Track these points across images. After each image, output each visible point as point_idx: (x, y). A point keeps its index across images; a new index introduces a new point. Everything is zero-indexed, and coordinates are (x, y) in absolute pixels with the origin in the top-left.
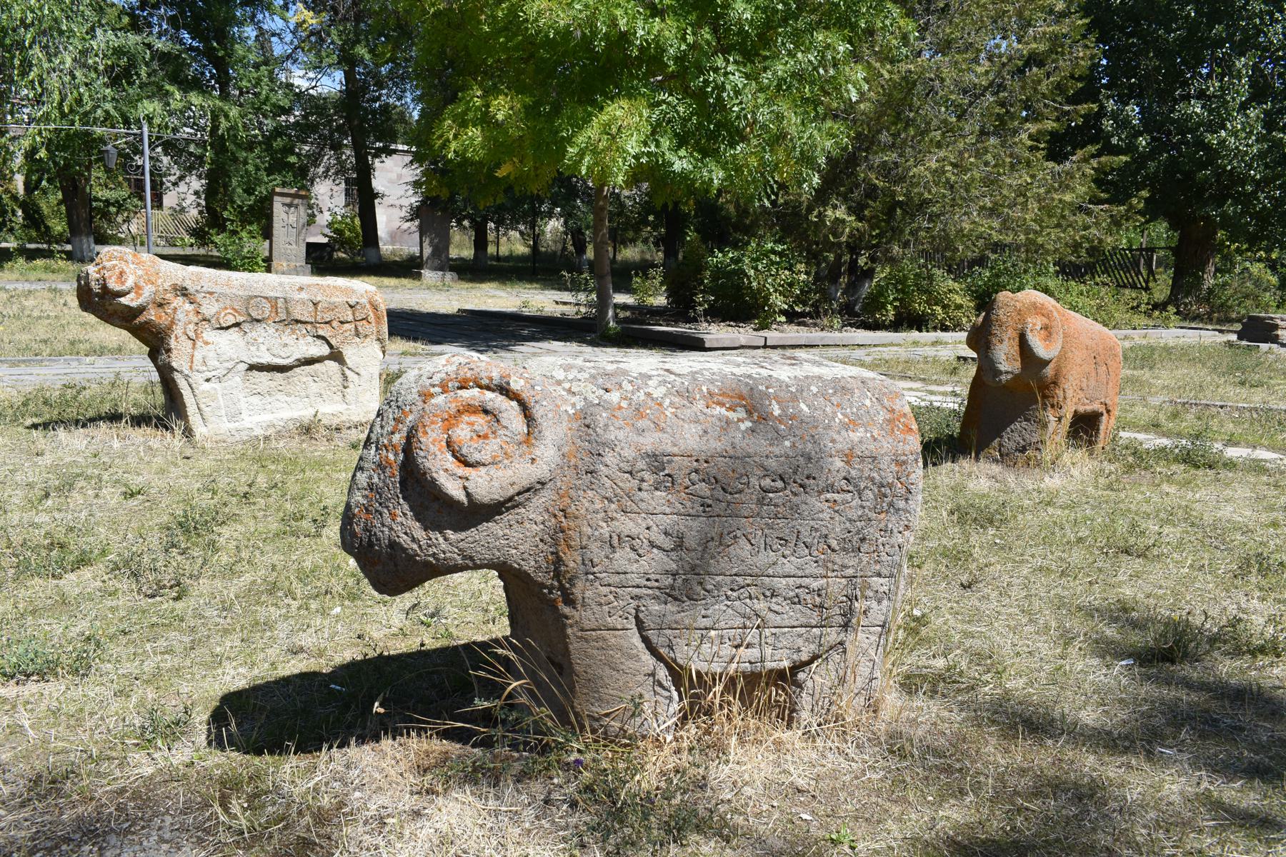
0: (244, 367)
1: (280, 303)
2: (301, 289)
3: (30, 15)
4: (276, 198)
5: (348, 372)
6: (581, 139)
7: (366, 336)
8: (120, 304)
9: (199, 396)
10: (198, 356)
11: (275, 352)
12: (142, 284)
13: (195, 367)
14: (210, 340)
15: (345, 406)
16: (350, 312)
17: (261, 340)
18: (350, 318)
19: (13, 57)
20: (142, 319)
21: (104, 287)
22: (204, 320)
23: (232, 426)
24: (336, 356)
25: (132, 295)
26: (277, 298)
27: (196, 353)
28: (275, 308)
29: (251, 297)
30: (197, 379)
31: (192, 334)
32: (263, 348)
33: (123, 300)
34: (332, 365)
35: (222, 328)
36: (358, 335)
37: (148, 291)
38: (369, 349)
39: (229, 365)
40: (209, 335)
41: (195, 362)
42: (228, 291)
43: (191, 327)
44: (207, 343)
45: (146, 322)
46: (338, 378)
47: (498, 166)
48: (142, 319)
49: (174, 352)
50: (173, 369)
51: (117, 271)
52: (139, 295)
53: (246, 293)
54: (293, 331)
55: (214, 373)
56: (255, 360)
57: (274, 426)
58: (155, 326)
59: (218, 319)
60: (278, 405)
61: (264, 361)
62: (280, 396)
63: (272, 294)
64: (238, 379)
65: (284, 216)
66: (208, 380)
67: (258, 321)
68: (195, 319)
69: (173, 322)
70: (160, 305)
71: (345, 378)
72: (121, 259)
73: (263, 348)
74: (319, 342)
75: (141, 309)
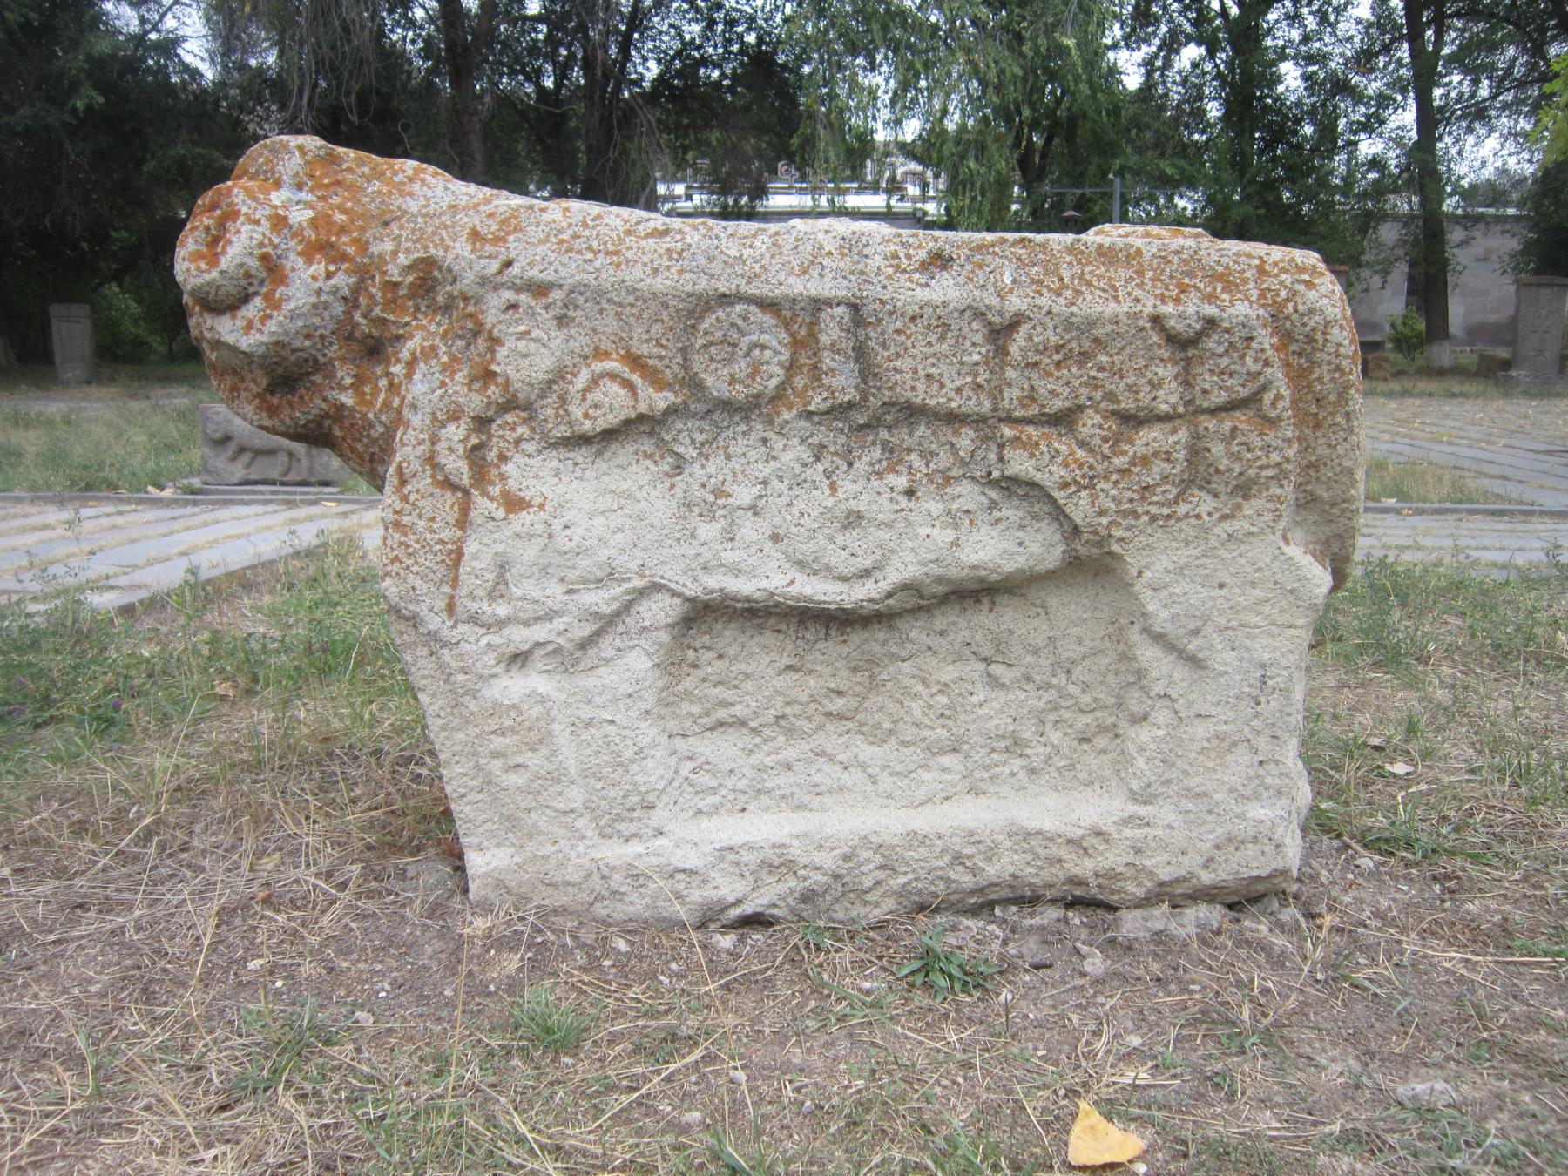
0: (660, 610)
1: (831, 331)
7: (1245, 489)
13: (466, 605)
16: (1166, 372)
17: (744, 494)
18: (1169, 398)
22: (510, 405)
23: (614, 853)
26: (817, 305)
27: (471, 547)
28: (804, 343)
35: (584, 440)
38: (1260, 552)
39: (602, 600)
41: (468, 582)
42: (609, 276)
44: (515, 504)
54: (894, 458)
55: (539, 633)
57: (790, 865)
59: (563, 400)
60: (827, 774)
62: (830, 739)
63: (798, 286)
66: (519, 659)
68: (474, 402)
73: (750, 530)
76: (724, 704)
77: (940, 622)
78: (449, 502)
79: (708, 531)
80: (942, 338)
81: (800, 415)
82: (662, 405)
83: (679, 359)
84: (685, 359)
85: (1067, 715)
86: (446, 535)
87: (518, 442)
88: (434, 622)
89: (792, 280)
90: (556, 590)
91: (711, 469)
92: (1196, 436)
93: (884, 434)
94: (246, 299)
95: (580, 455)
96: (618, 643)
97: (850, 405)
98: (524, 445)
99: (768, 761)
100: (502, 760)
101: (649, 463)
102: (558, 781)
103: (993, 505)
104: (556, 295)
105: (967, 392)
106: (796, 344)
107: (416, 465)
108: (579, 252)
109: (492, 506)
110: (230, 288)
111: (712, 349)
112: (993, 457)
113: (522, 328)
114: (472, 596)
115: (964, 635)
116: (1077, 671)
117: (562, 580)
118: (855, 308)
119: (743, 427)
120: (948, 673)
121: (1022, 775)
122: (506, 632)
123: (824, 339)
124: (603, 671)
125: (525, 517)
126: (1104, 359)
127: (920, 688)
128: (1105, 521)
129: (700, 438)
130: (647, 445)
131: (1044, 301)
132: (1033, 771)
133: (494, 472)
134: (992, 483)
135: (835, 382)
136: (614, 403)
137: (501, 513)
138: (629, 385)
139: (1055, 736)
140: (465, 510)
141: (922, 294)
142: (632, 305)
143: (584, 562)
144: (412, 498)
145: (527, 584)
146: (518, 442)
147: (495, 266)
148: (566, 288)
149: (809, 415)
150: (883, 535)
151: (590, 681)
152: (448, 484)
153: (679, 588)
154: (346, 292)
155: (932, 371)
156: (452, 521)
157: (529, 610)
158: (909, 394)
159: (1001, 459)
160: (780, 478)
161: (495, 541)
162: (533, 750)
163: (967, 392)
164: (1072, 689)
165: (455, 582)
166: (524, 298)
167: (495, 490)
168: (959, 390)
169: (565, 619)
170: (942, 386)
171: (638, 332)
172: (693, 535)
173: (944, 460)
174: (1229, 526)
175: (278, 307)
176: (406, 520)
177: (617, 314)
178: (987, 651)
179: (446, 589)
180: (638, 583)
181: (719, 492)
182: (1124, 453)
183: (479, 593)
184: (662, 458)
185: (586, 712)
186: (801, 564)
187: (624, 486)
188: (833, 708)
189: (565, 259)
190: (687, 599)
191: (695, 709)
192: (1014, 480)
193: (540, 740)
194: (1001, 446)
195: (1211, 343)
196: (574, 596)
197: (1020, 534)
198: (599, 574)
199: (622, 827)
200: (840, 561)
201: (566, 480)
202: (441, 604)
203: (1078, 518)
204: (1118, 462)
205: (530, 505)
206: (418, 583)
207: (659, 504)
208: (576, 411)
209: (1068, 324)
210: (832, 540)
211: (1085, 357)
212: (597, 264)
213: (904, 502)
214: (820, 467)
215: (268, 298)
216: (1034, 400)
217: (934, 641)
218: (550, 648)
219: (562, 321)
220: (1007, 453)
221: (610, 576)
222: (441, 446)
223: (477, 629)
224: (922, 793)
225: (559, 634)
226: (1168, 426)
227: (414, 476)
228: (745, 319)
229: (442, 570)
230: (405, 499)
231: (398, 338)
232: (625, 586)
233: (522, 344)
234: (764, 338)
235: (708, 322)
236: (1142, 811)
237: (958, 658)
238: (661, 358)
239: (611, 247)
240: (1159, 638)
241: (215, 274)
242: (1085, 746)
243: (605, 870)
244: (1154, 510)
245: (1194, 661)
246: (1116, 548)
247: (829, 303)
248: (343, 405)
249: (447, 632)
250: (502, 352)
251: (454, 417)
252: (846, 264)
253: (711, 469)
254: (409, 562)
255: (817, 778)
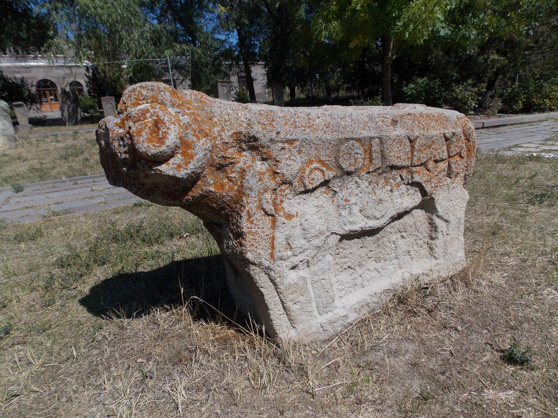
2: (394, 122)
3: (119, 18)
4: (219, 84)
5: (438, 221)
6: (406, 15)
8: (161, 175)
9: (286, 293)
10: (280, 237)
11: (369, 213)
12: (191, 138)
13: (277, 254)
14: (293, 212)
15: (434, 262)
19: (115, 36)
20: (196, 192)
21: (132, 149)
22: (284, 183)
24: (428, 205)
25: (178, 159)
26: (371, 138)
27: (277, 234)
28: (369, 152)
29: (341, 141)
30: (281, 268)
31: (269, 207)
32: (356, 209)
33: (163, 168)
34: (420, 214)
35: (307, 191)
36: (449, 175)
37: (201, 148)
40: (292, 204)
42: (312, 136)
43: (268, 196)
44: (289, 217)
45: (203, 196)
46: (425, 228)
47: (350, 41)
48: (196, 192)
49: (249, 237)
50: (248, 262)
51: (149, 120)
52: (188, 157)
53: (336, 136)
54: (387, 182)
55: (301, 257)
56: (349, 228)
58: (216, 200)
59: (302, 179)
61: (356, 228)
63: (365, 134)
64: (329, 258)
65: (222, 90)
66: (293, 268)
67: (349, 174)
68: (272, 184)
69: (241, 192)
70: (221, 168)
71: (433, 227)
72: (155, 100)
73: (356, 209)
74: (412, 190)
75: (194, 179)
76: (345, 264)
78: (268, 221)
79: (344, 213)
80: (400, 146)
81: (366, 173)
82: (332, 176)
83: (334, 160)
84: (336, 160)
85: (417, 241)
86: (268, 232)
87: (286, 195)
88: (267, 263)
89: (363, 132)
90: (303, 242)
91: (344, 194)
92: (449, 164)
93: (384, 175)
94: (172, 156)
95: (304, 196)
96: (323, 254)
97: (379, 168)
98: (288, 196)
99: (356, 276)
100: (293, 302)
101: (325, 195)
102: (309, 303)
104: (297, 143)
105: (406, 160)
106: (365, 151)
107: (254, 210)
108: (299, 127)
109: (283, 219)
110: (169, 151)
111: (344, 156)
112: (410, 177)
113: (287, 156)
114: (280, 251)
116: (420, 230)
117: (305, 238)
118: (380, 138)
119: (350, 179)
120: (393, 238)
121: (410, 260)
122: (290, 260)
123: (373, 149)
124: (319, 264)
125: (294, 220)
126: (434, 146)
127: (388, 244)
128: (432, 189)
129: (339, 184)
130: (323, 189)
131: (421, 132)
132: (412, 258)
133: (280, 207)
134: (408, 184)
135: (376, 162)
136: (319, 177)
137: (286, 221)
138: (322, 171)
139: (415, 247)
140: (274, 222)
141: (395, 133)
142: (320, 144)
143: (313, 232)
144: (255, 222)
145: (296, 242)
146: (286, 195)
147: (274, 135)
148: (300, 140)
149: (368, 173)
150: (387, 204)
151: (316, 268)
152: (266, 213)
153: (339, 233)
154: (211, 149)
155: (398, 155)
156: (269, 227)
157: (298, 250)
158: (393, 163)
159: (412, 177)
160: (361, 193)
161: (285, 231)
162: (302, 295)
163: (406, 160)
165: (273, 247)
166: (286, 145)
167: (281, 213)
168: (404, 160)
169: (309, 251)
170: (401, 159)
171: (323, 153)
172: (340, 215)
173: (399, 179)
174: (453, 185)
175: (192, 158)
176: (253, 230)
177: (316, 148)
178: (402, 230)
179: (270, 251)
180: (328, 234)
181: (347, 200)
182: (436, 171)
183: (282, 249)
184: (329, 193)
185: (316, 278)
186: (368, 217)
187: (321, 203)
188: (370, 256)
189: (296, 130)
190: (340, 235)
191: (338, 267)
193: (303, 291)
194: (412, 174)
195: (454, 140)
196: (310, 243)
197: (413, 197)
198: (317, 234)
199: (325, 310)
200: (378, 215)
201: (302, 205)
202: (268, 257)
204: (436, 173)
205: (294, 216)
206: (261, 251)
207: (330, 207)
208: (307, 182)
209: (428, 138)
210: (375, 208)
211: (430, 146)
212: (307, 131)
213: (389, 193)
214: (371, 188)
215: (183, 154)
216: (419, 159)
218: (305, 261)
219: (300, 152)
220: (414, 175)
221: (321, 233)
222: (264, 201)
223: (281, 261)
225: (308, 256)
226: (444, 162)
227: (254, 214)
228: (353, 145)
229: (268, 245)
230: (252, 222)
231: (231, 163)
232: (324, 235)
233: (288, 162)
234: (358, 151)
235: (343, 148)
237: (396, 233)
238: (329, 161)
239: (308, 125)
241: (164, 148)
242: (421, 248)
243: (323, 325)
244: (441, 184)
245: (446, 221)
246: (433, 196)
247: (373, 138)
248: (210, 191)
249: (272, 266)
250: (280, 165)
251: (266, 191)
252: (374, 126)
253: (344, 194)
254: (257, 245)
255: (368, 277)
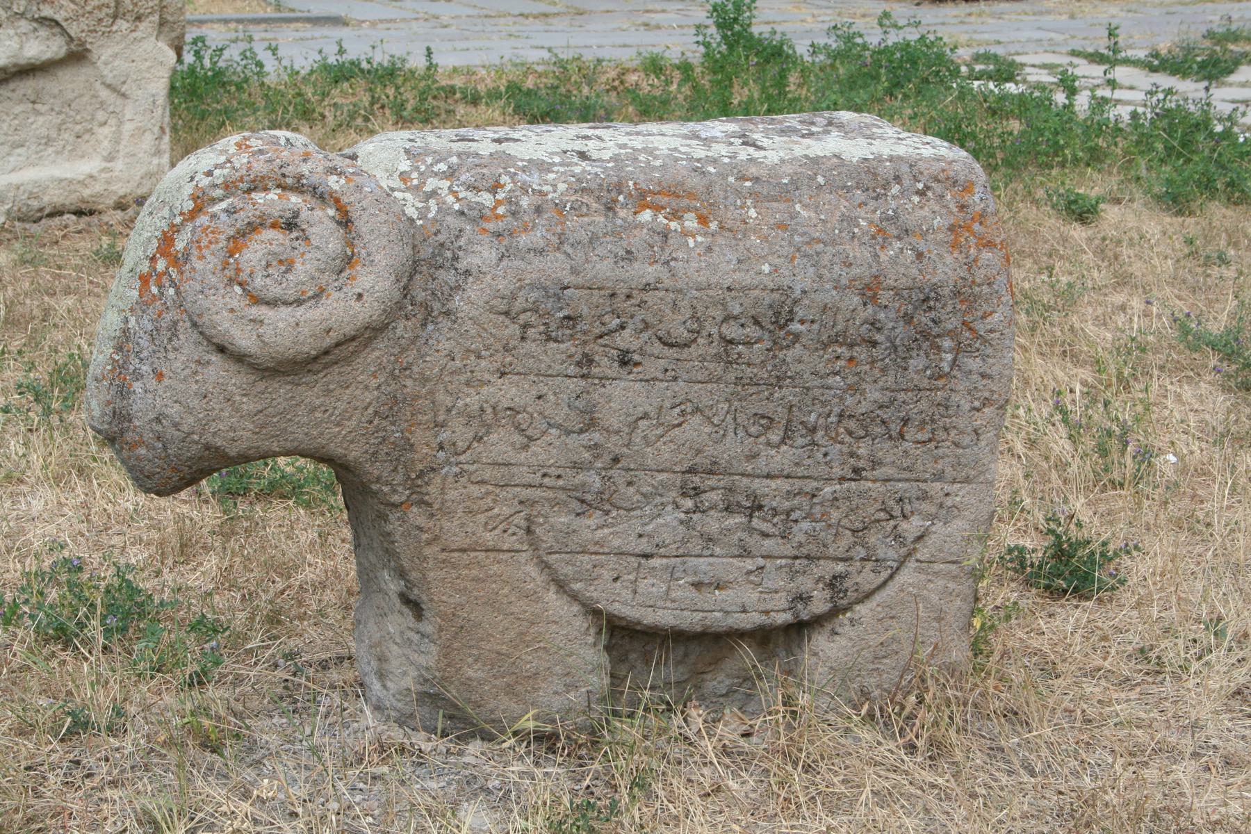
77: (12, 85)
85: (70, 125)
103: (35, 30)
112: (35, 8)
115: (22, 92)
120: (18, 109)
134: (36, 20)
164: (72, 113)
174: (134, 35)
192: (45, 19)
203: (73, 35)
204: (88, 8)
217: (9, 94)
224: (10, 168)
236: (109, 165)
237: (21, 101)
240: (109, 86)
245: (124, 95)
246: (88, 46)
